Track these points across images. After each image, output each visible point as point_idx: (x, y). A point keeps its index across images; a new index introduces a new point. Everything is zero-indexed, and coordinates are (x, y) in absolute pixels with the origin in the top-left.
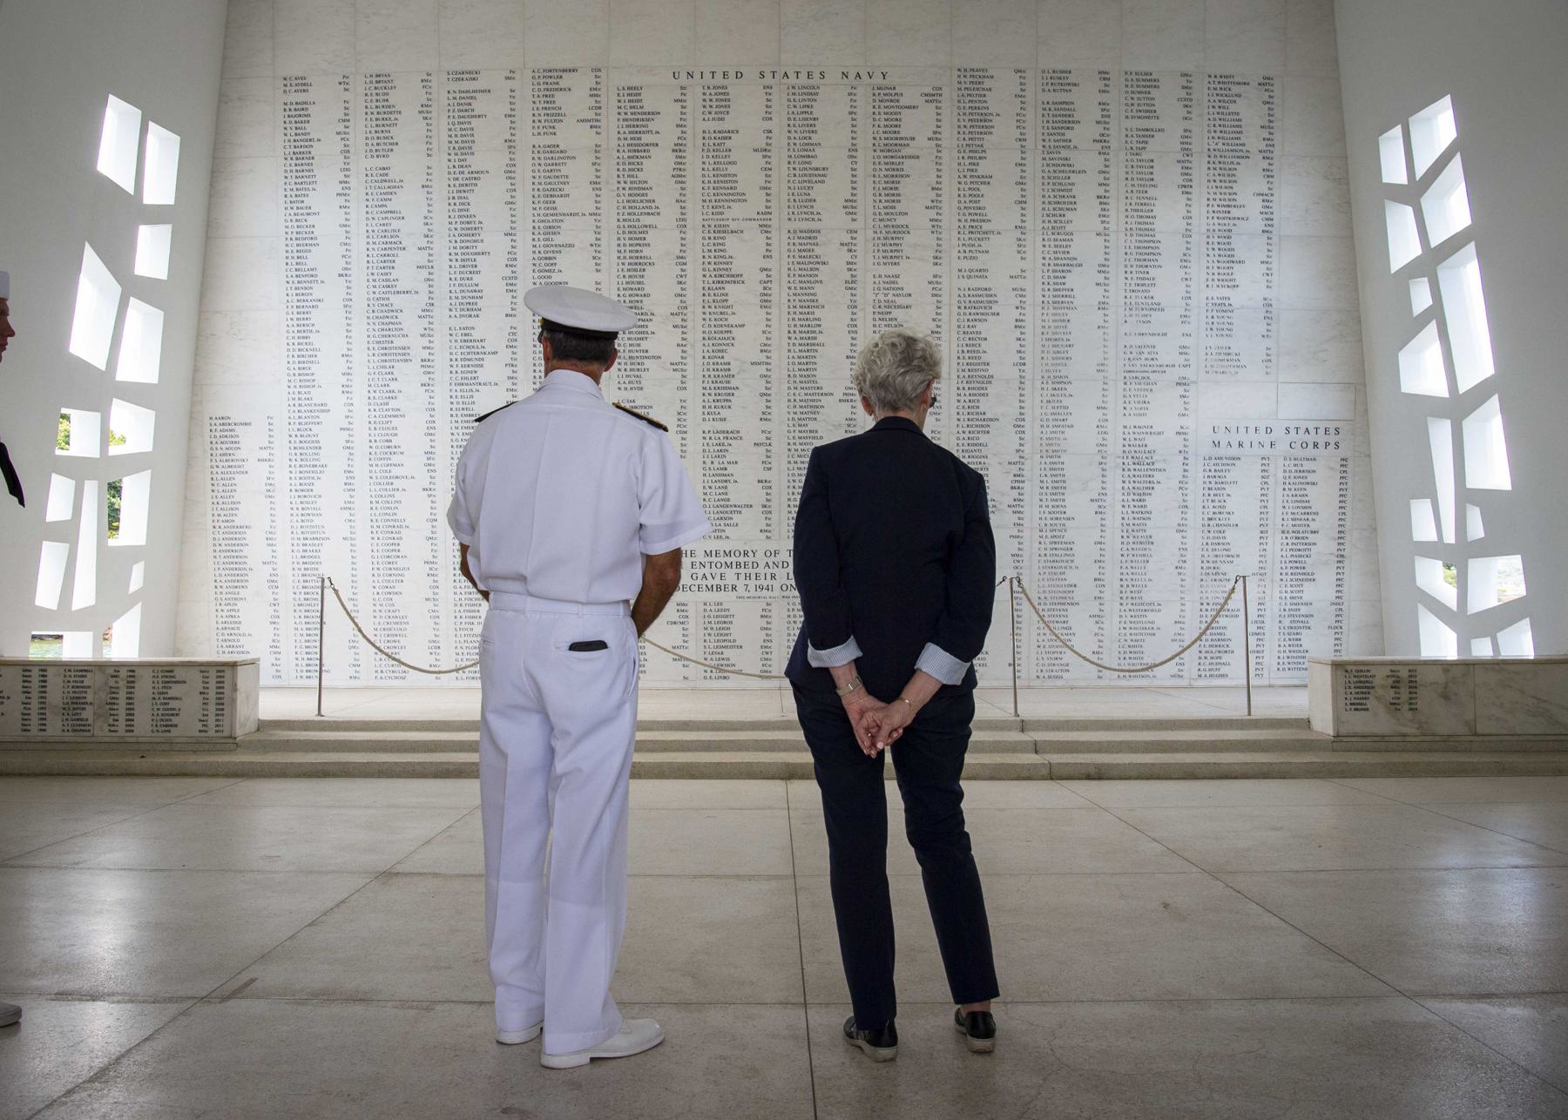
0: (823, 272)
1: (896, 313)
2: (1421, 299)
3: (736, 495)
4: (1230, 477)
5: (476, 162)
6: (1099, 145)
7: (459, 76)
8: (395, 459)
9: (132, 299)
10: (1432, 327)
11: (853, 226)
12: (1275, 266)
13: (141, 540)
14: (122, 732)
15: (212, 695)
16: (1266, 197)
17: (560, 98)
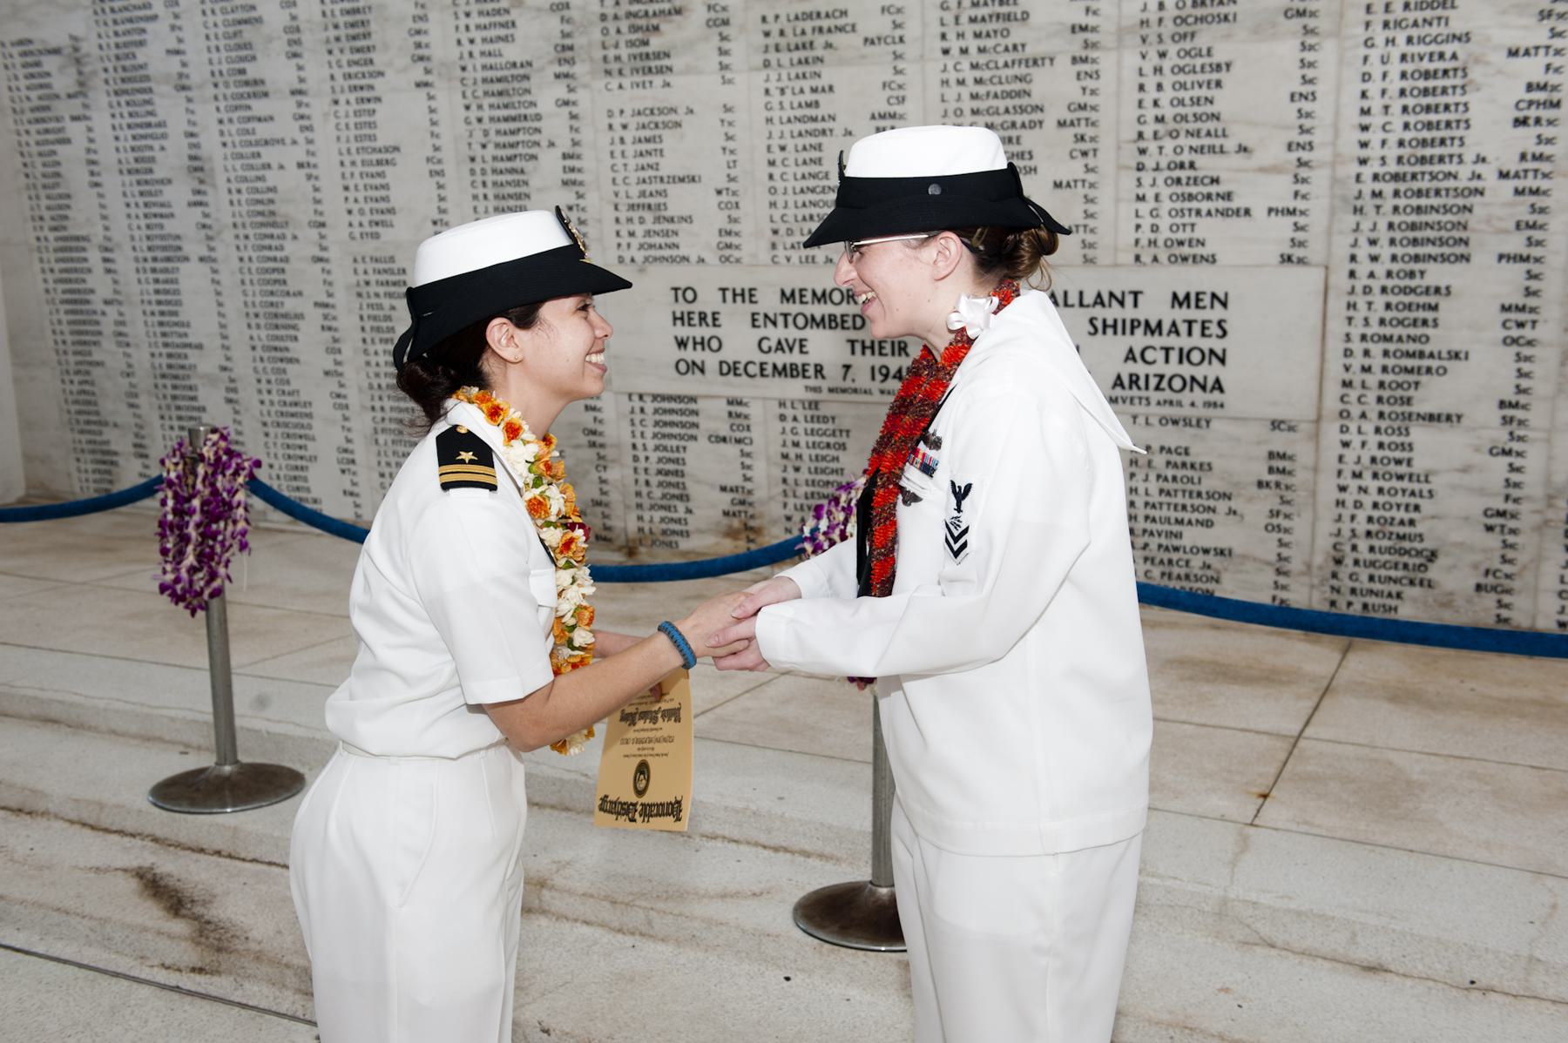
8: (259, 107)
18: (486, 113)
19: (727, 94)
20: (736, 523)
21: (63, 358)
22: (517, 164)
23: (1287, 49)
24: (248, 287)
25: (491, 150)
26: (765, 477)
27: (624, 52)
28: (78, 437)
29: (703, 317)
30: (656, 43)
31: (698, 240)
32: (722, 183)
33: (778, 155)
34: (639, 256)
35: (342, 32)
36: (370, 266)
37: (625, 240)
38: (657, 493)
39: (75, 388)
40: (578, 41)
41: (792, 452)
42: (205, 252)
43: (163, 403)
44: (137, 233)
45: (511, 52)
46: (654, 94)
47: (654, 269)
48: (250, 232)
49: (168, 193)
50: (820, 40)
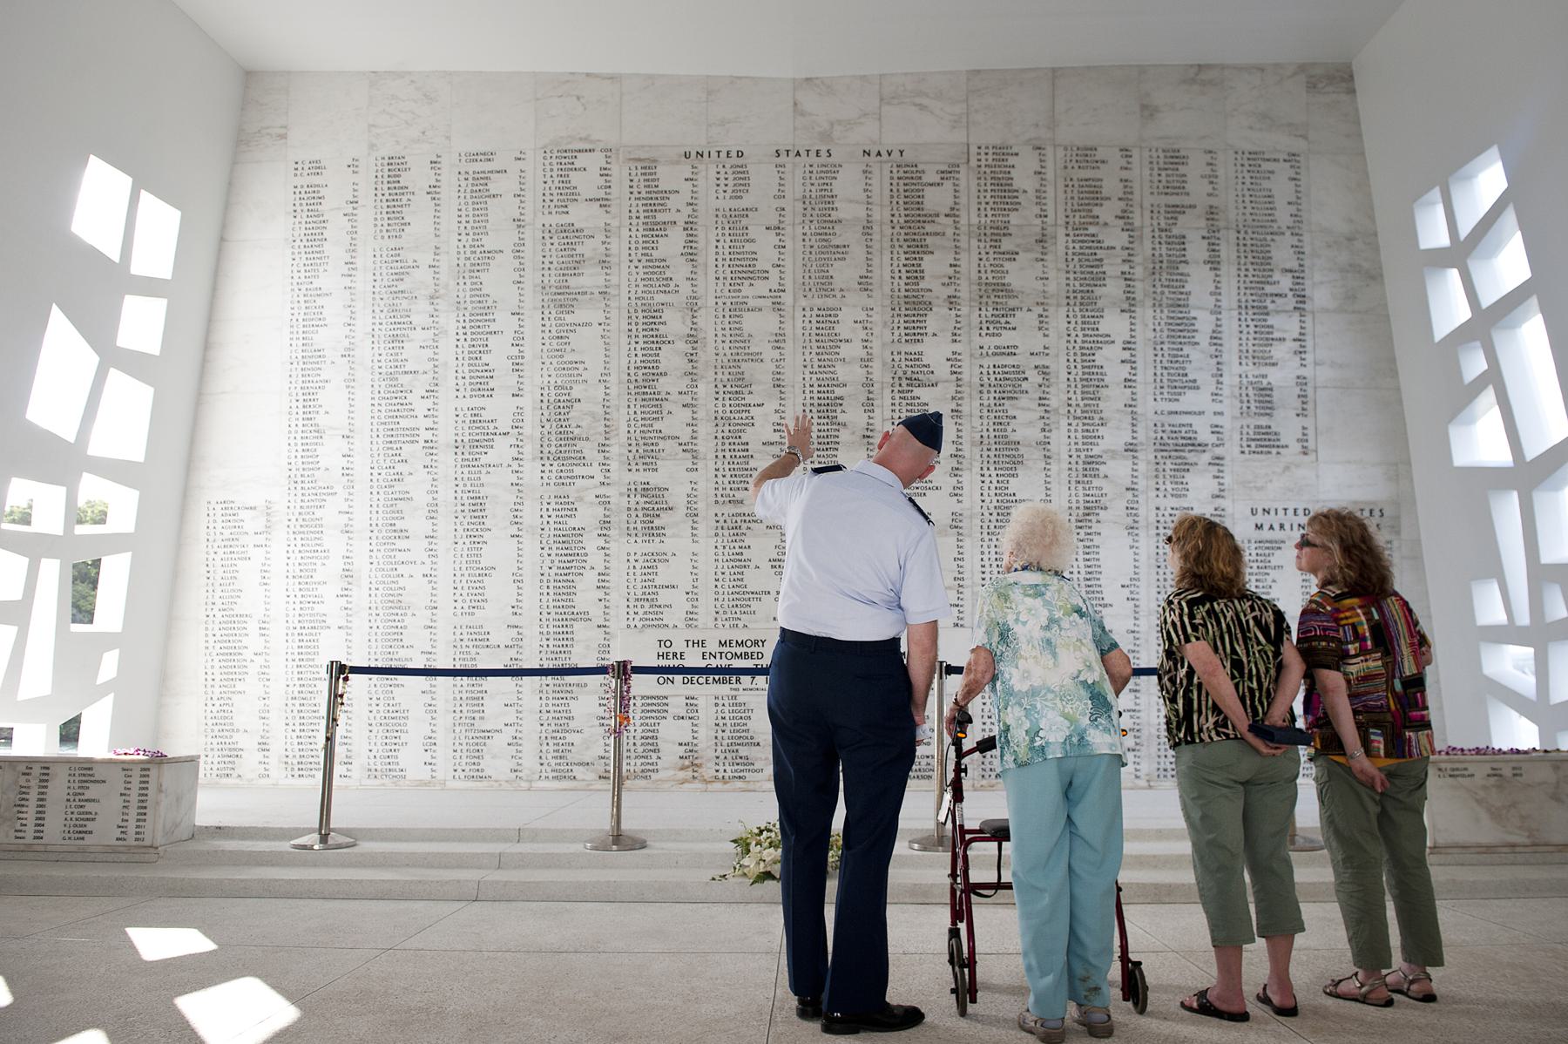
0: (845, 350)
1: (917, 392)
2: (1474, 364)
3: (753, 580)
4: (1274, 561)
5: (489, 243)
6: (1121, 222)
7: (474, 157)
8: (400, 544)
9: (112, 370)
10: (1488, 396)
11: (870, 303)
12: (1309, 344)
13: (117, 627)
14: (29, 839)
15: (134, 797)
16: (1297, 275)
17: (575, 177)
18: (553, 552)
19: (695, 548)
20: (687, 762)
21: (209, 690)
22: (570, 578)
23: (952, 540)
24: (373, 644)
25: (555, 570)
26: (705, 735)
27: (639, 526)
28: (209, 740)
29: (675, 655)
30: (657, 522)
31: (674, 616)
32: (690, 589)
33: (720, 576)
34: (639, 625)
35: (466, 508)
36: (465, 631)
37: (632, 616)
38: (640, 749)
39: (214, 709)
40: (612, 519)
41: (721, 722)
42: (344, 623)
43: (290, 715)
44: (291, 613)
45: (572, 523)
46: (655, 546)
47: (649, 630)
48: (380, 611)
49: (321, 589)
50: (744, 526)
